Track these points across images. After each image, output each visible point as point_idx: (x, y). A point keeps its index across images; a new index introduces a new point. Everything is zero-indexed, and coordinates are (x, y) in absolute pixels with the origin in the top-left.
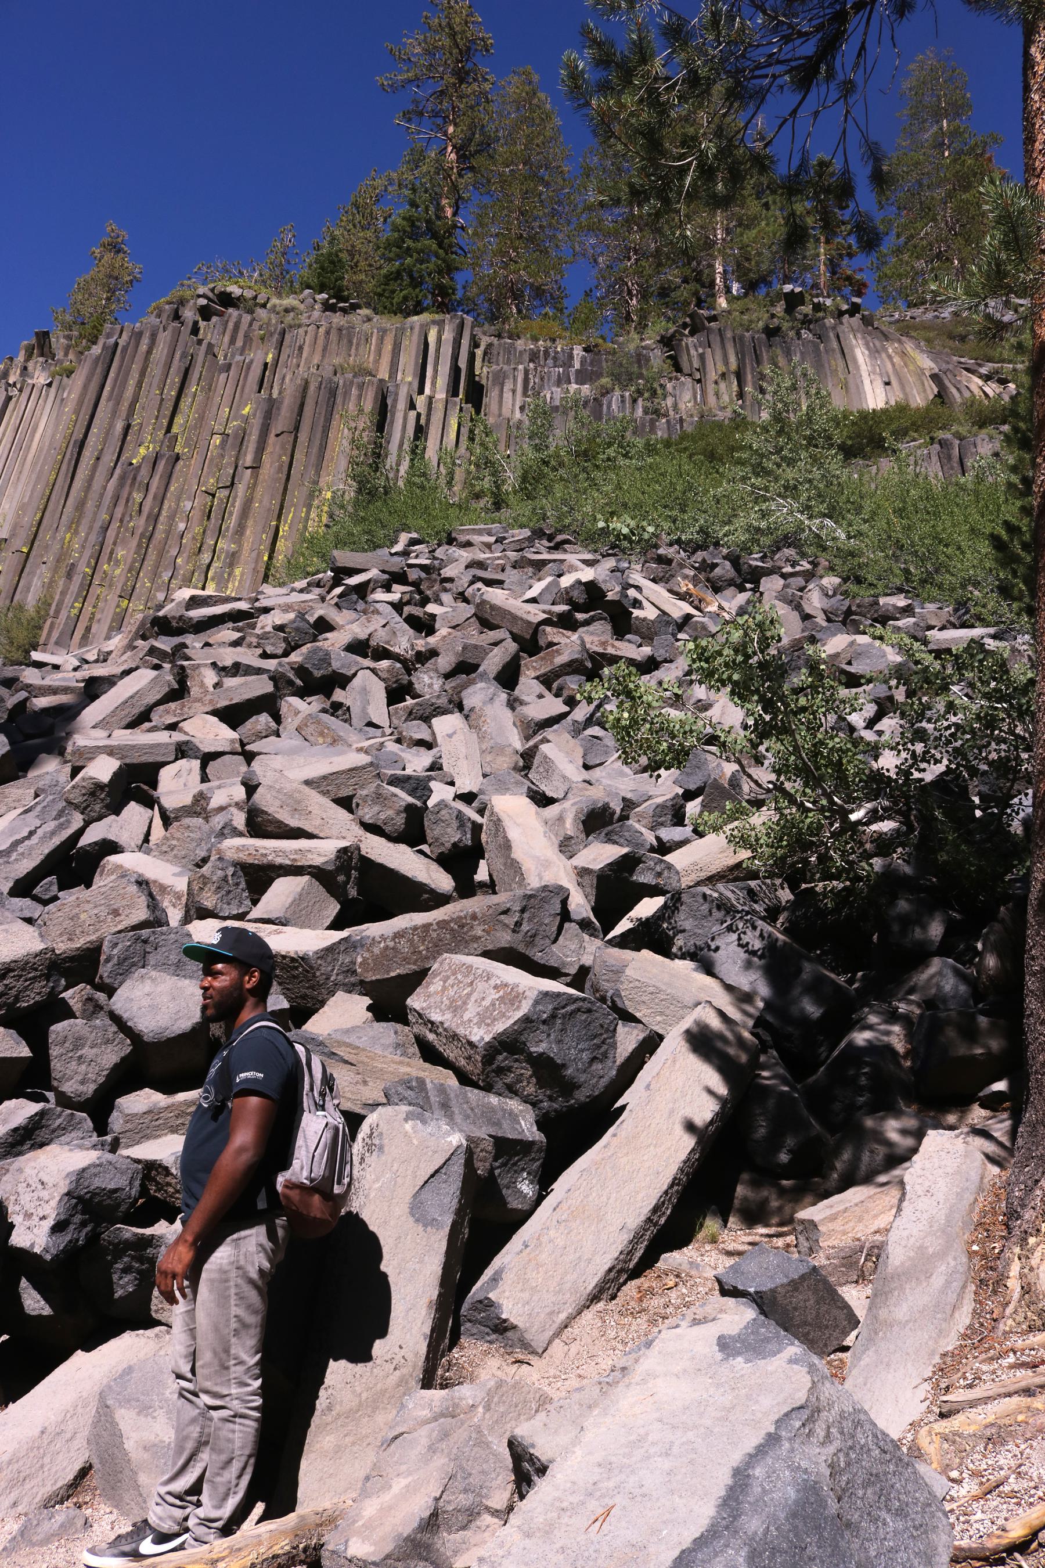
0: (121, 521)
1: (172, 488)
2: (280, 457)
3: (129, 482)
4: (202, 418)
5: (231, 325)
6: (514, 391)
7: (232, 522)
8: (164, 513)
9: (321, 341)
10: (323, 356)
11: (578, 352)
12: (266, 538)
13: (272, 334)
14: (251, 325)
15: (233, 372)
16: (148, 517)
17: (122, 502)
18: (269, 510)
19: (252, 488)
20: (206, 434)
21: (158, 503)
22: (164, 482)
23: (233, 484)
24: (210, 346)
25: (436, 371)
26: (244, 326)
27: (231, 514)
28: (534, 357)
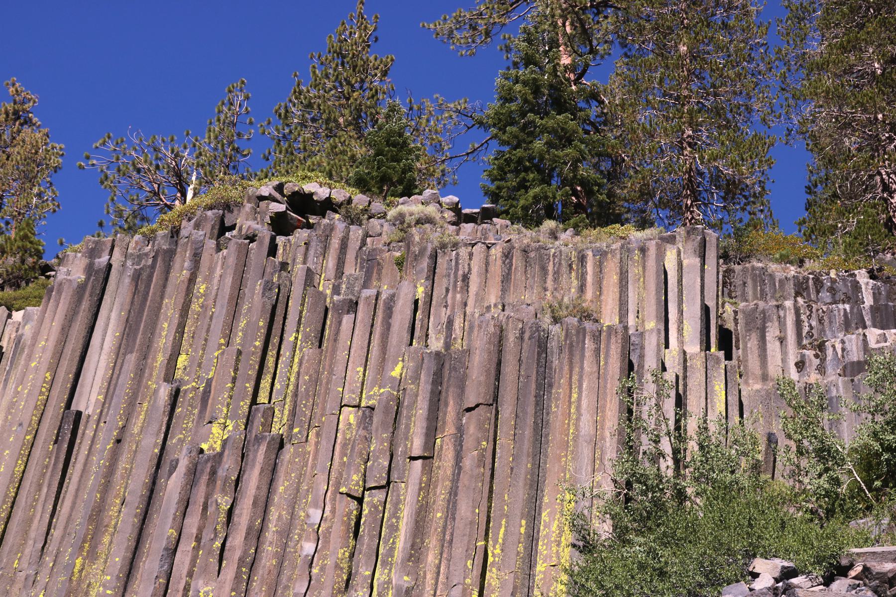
0: (198, 539)
1: (281, 489)
2: (479, 443)
3: (205, 478)
4: (316, 381)
5: (335, 243)
6: (782, 340)
7: (401, 542)
8: (272, 527)
9: (497, 268)
10: (504, 291)
11: (862, 277)
12: (472, 566)
13: (416, 258)
14: (364, 243)
15: (363, 310)
16: (248, 534)
17: (195, 511)
18: (471, 523)
19: (426, 488)
20: (331, 405)
21: (260, 510)
22: (266, 480)
23: (389, 483)
24: (309, 274)
25: (681, 312)
26: (354, 244)
27: (394, 529)
28: (801, 288)
